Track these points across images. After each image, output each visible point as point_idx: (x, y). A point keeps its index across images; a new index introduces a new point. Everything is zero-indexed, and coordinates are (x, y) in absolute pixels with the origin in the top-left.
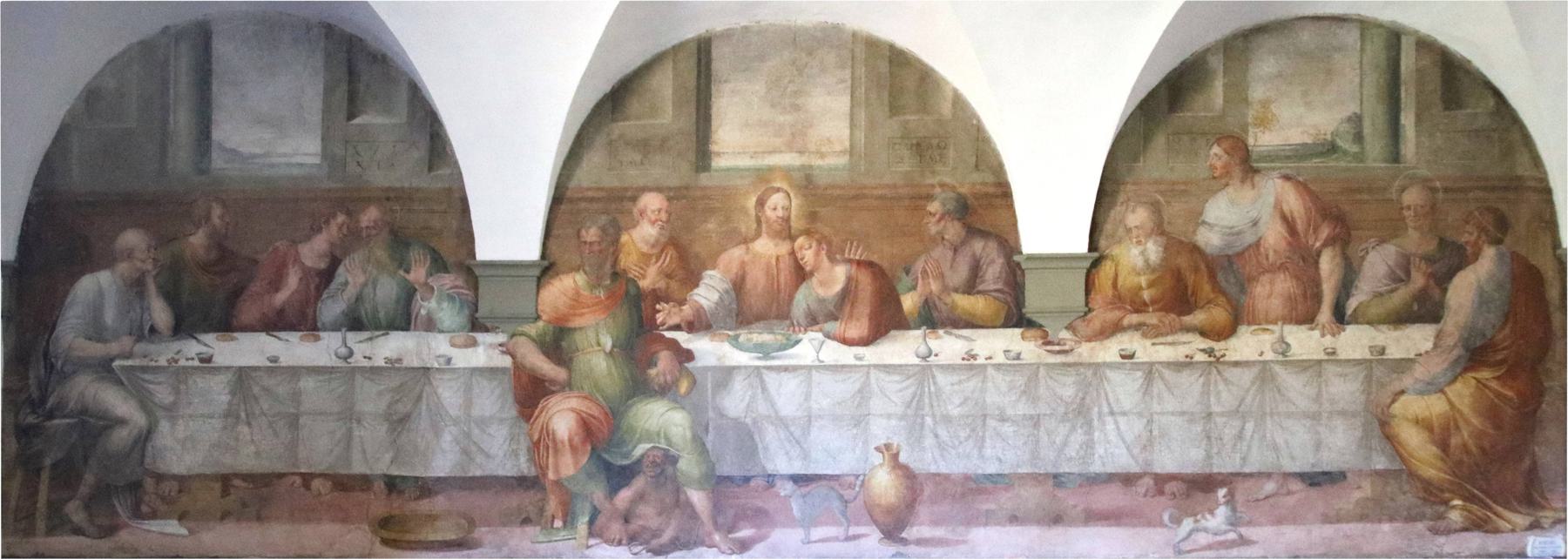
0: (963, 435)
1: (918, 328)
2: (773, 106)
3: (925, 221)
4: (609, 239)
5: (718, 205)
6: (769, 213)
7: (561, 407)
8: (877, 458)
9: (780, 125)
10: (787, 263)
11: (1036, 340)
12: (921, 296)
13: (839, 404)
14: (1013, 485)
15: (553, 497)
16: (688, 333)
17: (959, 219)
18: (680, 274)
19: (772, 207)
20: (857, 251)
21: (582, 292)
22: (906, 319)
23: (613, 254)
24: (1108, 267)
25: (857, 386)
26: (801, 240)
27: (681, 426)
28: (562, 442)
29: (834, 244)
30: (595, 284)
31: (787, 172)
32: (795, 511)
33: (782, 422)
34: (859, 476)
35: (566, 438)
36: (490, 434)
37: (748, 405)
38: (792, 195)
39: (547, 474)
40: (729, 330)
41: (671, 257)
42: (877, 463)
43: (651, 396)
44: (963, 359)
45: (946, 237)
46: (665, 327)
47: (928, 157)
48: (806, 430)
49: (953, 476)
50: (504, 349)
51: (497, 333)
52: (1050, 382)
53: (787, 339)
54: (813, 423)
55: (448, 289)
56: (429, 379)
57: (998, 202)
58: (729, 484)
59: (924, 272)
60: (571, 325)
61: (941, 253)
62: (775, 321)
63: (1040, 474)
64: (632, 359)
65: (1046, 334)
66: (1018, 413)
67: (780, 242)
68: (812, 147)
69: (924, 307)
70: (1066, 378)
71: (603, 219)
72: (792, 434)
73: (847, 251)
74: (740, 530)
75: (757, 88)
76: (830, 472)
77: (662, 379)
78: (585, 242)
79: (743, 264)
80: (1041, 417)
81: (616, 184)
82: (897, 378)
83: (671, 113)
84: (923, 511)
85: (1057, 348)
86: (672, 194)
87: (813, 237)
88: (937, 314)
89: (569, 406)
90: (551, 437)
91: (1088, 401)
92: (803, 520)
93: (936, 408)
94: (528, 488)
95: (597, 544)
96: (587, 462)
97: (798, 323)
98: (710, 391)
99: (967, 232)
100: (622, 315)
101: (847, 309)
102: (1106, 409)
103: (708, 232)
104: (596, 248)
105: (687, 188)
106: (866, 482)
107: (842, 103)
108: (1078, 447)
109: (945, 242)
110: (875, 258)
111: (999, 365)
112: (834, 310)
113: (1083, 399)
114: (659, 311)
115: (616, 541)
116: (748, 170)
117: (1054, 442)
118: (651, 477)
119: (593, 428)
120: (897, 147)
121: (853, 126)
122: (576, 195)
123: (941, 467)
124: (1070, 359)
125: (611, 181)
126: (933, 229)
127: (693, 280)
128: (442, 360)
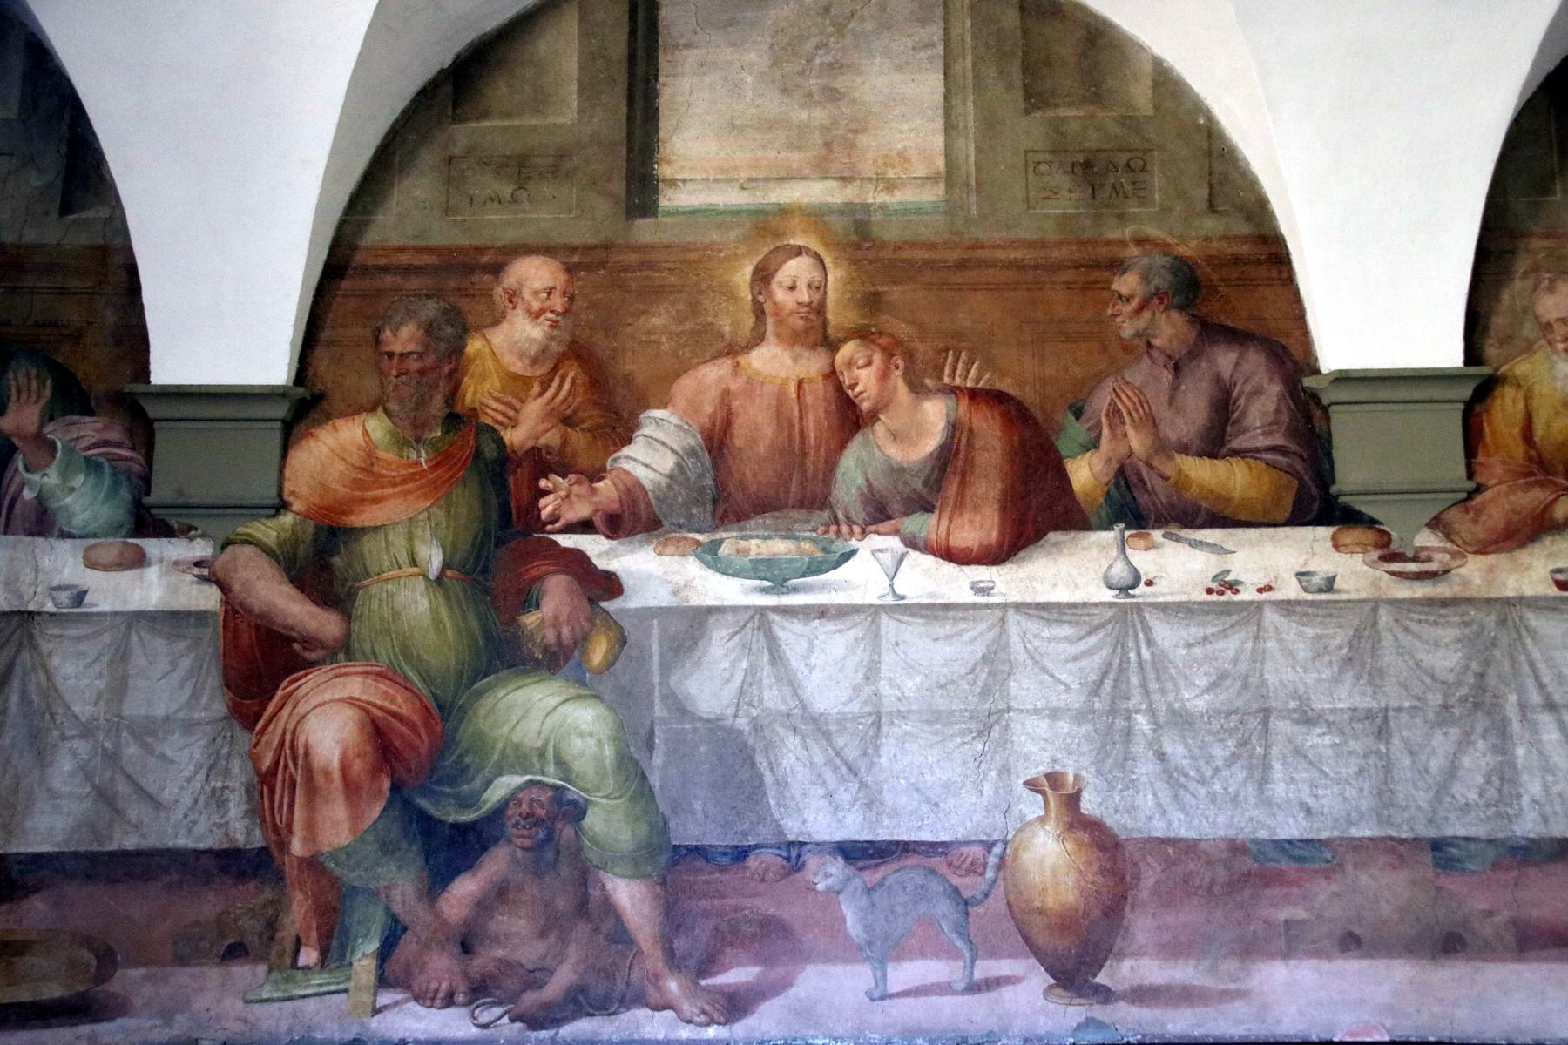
0: (1219, 753)
1: (1108, 526)
2: (784, 91)
3: (1109, 312)
4: (443, 346)
5: (673, 280)
6: (780, 295)
7: (327, 696)
8: (1031, 806)
9: (799, 127)
10: (821, 393)
11: (1365, 552)
12: (1109, 460)
13: (942, 687)
14: (1341, 865)
15: (299, 896)
16: (608, 537)
17: (1182, 308)
18: (591, 416)
19: (789, 283)
20: (968, 371)
21: (382, 454)
22: (1080, 511)
23: (450, 375)
24: (1508, 401)
25: (980, 649)
26: (848, 350)
27: (591, 735)
28: (327, 773)
29: (920, 356)
30: (410, 434)
31: (815, 217)
32: (849, 924)
33: (817, 726)
34: (994, 844)
35: (336, 763)
36: (163, 757)
37: (741, 692)
38: (828, 261)
39: (290, 843)
40: (698, 531)
41: (573, 382)
42: (1030, 817)
43: (525, 673)
44: (1210, 591)
45: (1157, 342)
46: (557, 525)
47: (1108, 188)
48: (871, 745)
49: (1203, 846)
50: (206, 572)
51: (191, 539)
52: (1406, 640)
53: (824, 550)
54: (885, 729)
55: (88, 448)
56: (31, 637)
57: (1262, 272)
58: (700, 863)
59: (1114, 413)
60: (357, 520)
61: (1147, 376)
62: (795, 514)
63: (1403, 841)
64: (486, 591)
65: (1384, 540)
66: (1341, 705)
67: (806, 353)
68: (868, 169)
69: (1117, 485)
70: (1440, 631)
71: (430, 309)
72: (838, 754)
73: (947, 371)
74: (724, 969)
75: (753, 56)
76: (926, 836)
77: (551, 637)
78: (391, 355)
79: (726, 394)
80: (1391, 714)
81: (463, 241)
82: (1066, 631)
83: (575, 104)
84: (1142, 925)
85: (1412, 567)
86: (576, 259)
87: (873, 341)
88: (1146, 496)
89: (345, 694)
90: (300, 762)
91: (1492, 680)
92: (870, 944)
93: (1157, 697)
94: (242, 877)
95: (396, 1004)
96: (380, 817)
97: (848, 518)
98: (656, 659)
99: (1199, 335)
100: (466, 500)
101: (952, 488)
102: (1535, 698)
103: (649, 333)
104: (414, 365)
105: (607, 247)
106: (1009, 859)
107: (930, 86)
108: (1480, 780)
109: (1155, 353)
110: (1006, 385)
111: (1289, 602)
112: (924, 491)
113: (1481, 675)
114: (545, 493)
115: (441, 995)
116: (736, 212)
117: (1427, 771)
118: (524, 849)
119: (397, 743)
120: (1044, 168)
121: (950, 127)
122: (370, 262)
123: (1176, 824)
124: (1442, 590)
125: (444, 234)
126: (1128, 330)
127: (620, 430)
128: (64, 597)
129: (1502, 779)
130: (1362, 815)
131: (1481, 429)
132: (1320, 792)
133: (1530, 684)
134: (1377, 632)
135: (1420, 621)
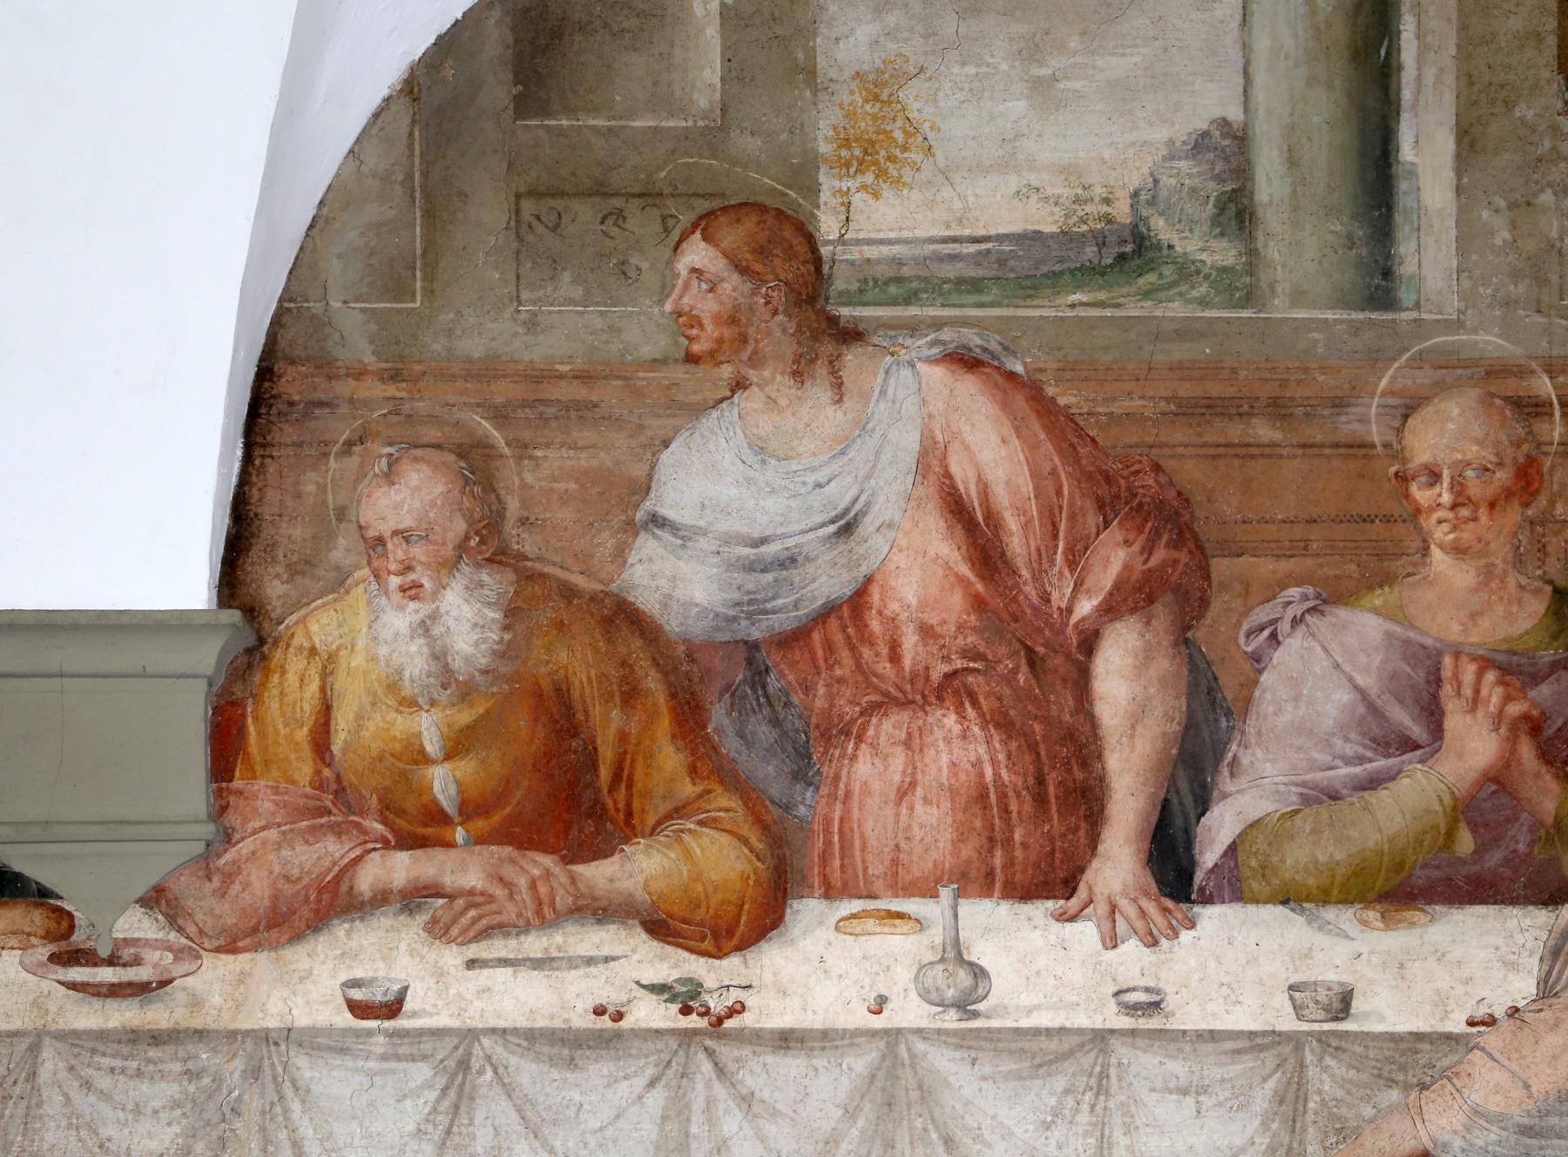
24: (292, 679)
52: (84, 1102)
65: (62, 924)
85: (107, 975)
131: (242, 729)
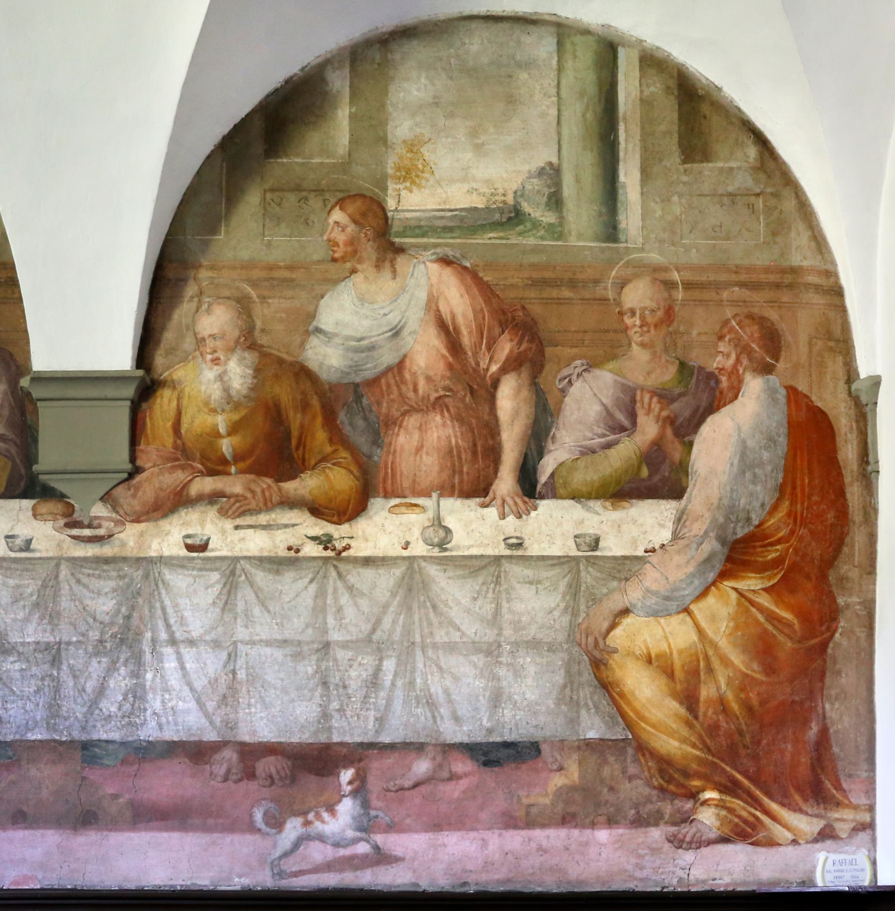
14: (19, 760)
24: (166, 400)
52: (77, 588)
65: (70, 510)
80: (63, 646)
85: (87, 532)
91: (135, 621)
102: (163, 636)
113: (128, 618)
117: (84, 690)
124: (107, 550)
129: (135, 697)
130: (36, 723)
132: (9, 706)
133: (161, 624)
134: (58, 583)
135: (89, 575)
